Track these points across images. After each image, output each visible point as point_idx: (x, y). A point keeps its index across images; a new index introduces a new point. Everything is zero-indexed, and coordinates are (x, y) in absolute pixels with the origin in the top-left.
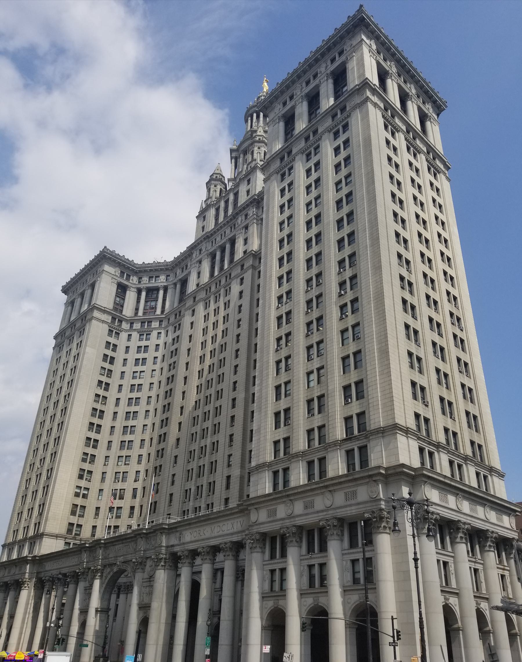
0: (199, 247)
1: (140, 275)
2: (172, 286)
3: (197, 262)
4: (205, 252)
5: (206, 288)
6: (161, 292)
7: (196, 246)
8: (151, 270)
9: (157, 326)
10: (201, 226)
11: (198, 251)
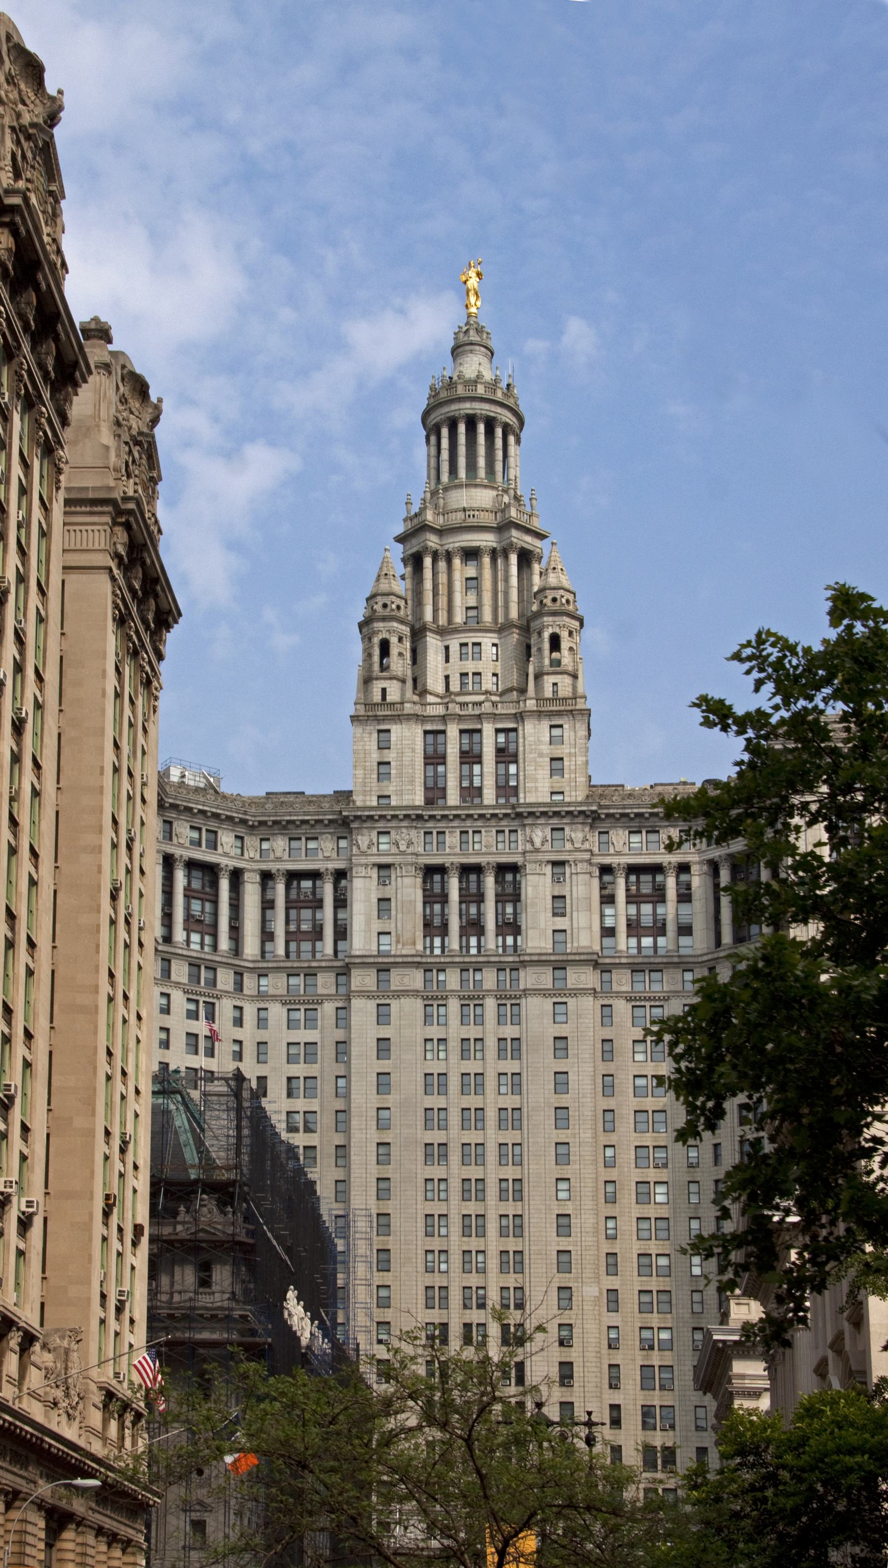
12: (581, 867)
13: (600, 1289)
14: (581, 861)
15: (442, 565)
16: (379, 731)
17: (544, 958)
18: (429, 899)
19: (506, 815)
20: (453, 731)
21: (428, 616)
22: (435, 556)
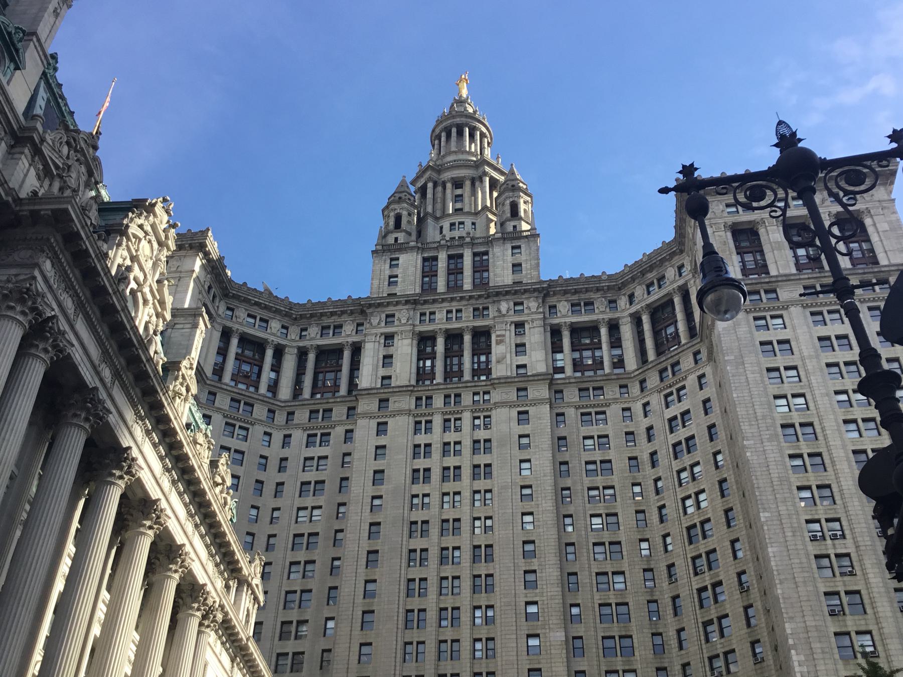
0: (390, 310)
1: (234, 303)
2: (296, 351)
3: (382, 334)
4: (405, 325)
5: (419, 394)
6: (269, 353)
7: (380, 305)
8: (257, 304)
9: (264, 418)
10: (388, 272)
11: (383, 316)
12: (536, 323)
13: (566, 636)
14: (536, 320)
15: (439, 189)
16: (392, 260)
17: (509, 380)
18: (422, 355)
19: (480, 296)
20: (442, 256)
21: (430, 209)
22: (435, 185)
